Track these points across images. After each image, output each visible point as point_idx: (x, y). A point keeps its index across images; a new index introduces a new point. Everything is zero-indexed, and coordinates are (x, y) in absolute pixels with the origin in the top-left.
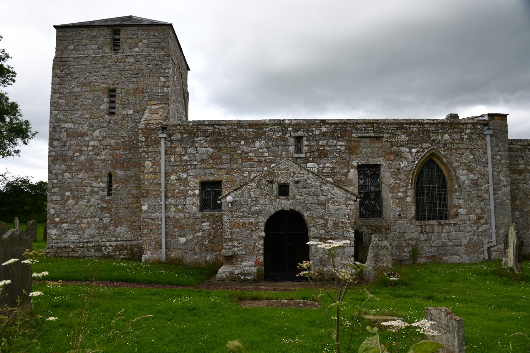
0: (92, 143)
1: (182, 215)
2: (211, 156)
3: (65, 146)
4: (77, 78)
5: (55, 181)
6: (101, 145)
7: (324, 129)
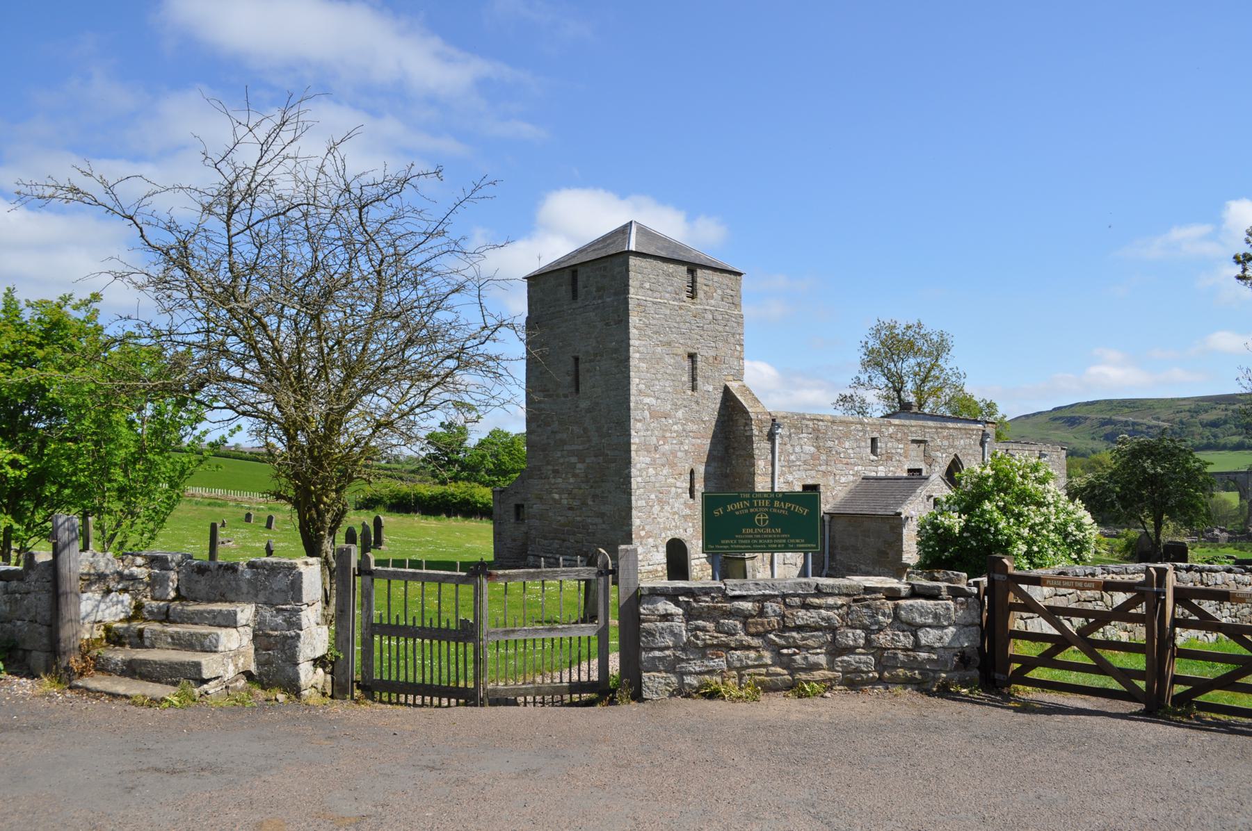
0: (675, 427)
2: (812, 455)
5: (639, 479)
7: (891, 430)
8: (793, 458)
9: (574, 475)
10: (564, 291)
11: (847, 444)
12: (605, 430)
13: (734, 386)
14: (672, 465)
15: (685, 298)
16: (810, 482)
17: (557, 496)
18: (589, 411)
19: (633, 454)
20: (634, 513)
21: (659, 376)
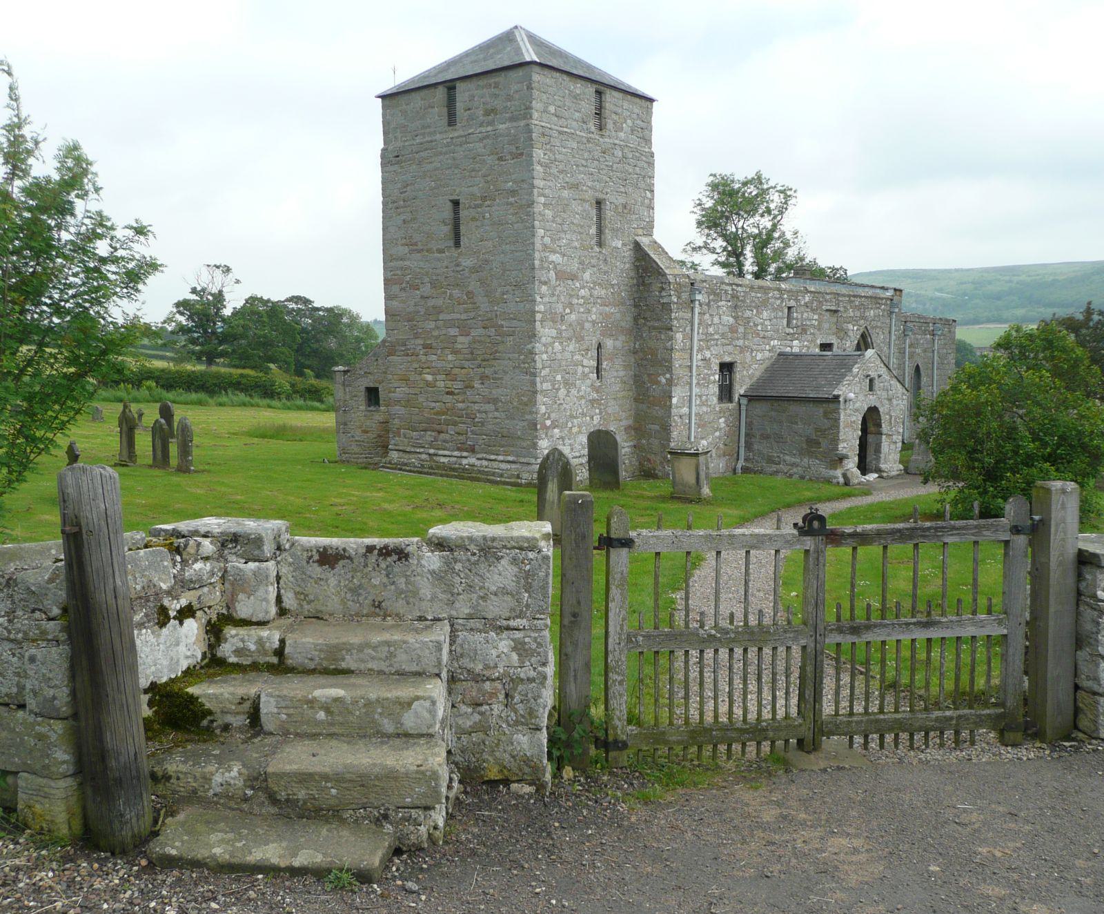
0: (582, 292)
1: (705, 409)
3: (554, 295)
4: (561, 172)
5: (545, 356)
6: (591, 296)
8: (711, 330)
9: (455, 352)
10: (437, 114)
11: (765, 314)
12: (497, 295)
13: (644, 241)
14: (580, 339)
15: (593, 129)
16: (727, 359)
17: (429, 378)
18: (475, 270)
19: (538, 324)
20: (539, 397)
21: (565, 227)
